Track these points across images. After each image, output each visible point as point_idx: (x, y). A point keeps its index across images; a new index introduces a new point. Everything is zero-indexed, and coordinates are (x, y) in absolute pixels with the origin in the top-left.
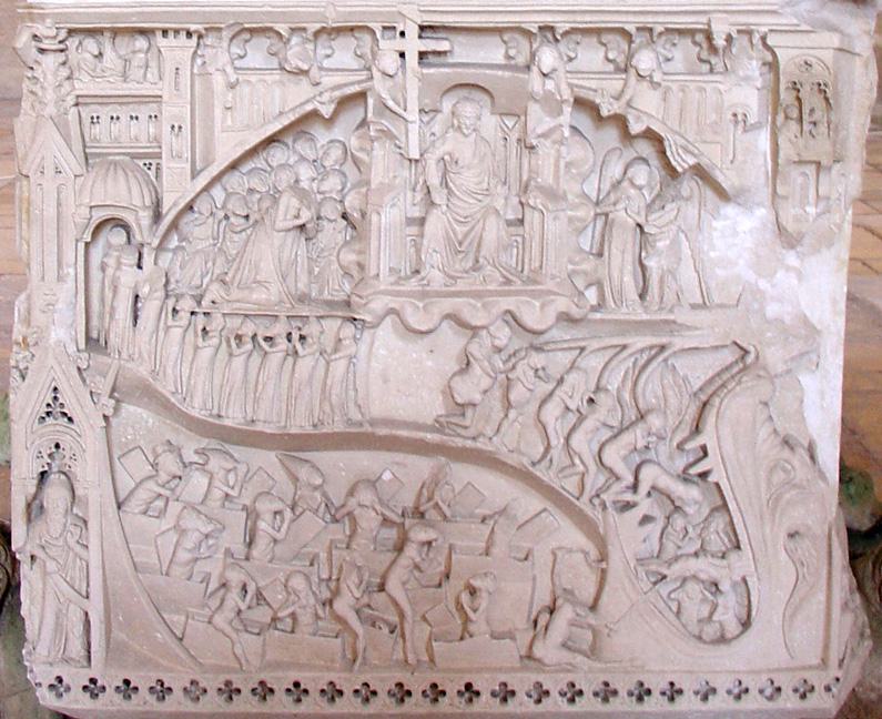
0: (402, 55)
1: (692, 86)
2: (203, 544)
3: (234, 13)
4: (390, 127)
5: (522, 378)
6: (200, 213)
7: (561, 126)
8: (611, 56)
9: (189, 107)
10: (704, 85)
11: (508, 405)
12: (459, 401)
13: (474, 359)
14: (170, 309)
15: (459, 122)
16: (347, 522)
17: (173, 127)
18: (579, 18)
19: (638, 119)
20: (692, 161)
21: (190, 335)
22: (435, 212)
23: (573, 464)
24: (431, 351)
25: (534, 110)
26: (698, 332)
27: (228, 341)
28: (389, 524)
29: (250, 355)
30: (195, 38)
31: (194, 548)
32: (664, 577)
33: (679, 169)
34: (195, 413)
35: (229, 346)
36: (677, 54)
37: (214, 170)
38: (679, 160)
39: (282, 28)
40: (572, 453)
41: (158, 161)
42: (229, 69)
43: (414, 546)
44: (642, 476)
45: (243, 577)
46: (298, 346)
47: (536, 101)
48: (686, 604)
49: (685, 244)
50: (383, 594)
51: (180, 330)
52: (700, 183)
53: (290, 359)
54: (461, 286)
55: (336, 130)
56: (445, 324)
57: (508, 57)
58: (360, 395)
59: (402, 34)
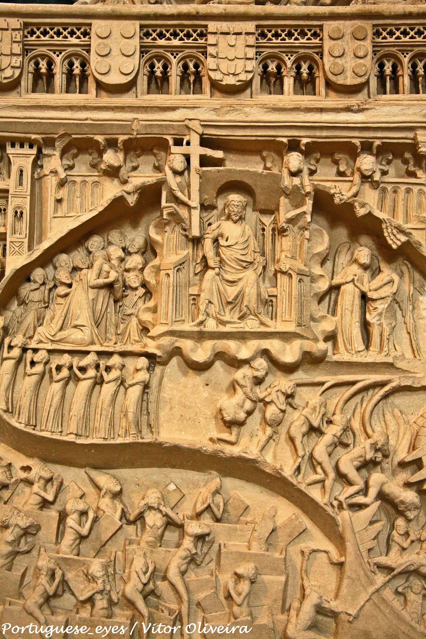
0: (187, 158)
1: (403, 188)
2: (23, 541)
3: (64, 124)
4: (177, 208)
5: (276, 401)
6: (35, 282)
7: (305, 213)
8: (342, 169)
9: (29, 198)
10: (411, 186)
11: (265, 421)
12: (228, 418)
13: (238, 384)
14: (6, 346)
15: (229, 210)
16: (139, 526)
17: (16, 212)
18: (318, 133)
19: (363, 205)
20: (403, 239)
21: (21, 368)
22: (210, 273)
23: (316, 472)
24: (207, 385)
25: (283, 201)
26: (411, 375)
27: (51, 369)
28: (172, 527)
29: (67, 384)
30: (34, 151)
31: (14, 541)
32: (393, 569)
33: (394, 247)
34: (21, 427)
35: (51, 377)
36: (392, 170)
37: (46, 245)
38: (394, 240)
39: (100, 138)
40: (315, 463)
41: (4, 242)
42: (61, 170)
43: (192, 539)
44: (371, 483)
45: (52, 565)
46: (104, 374)
47: (287, 196)
48: (411, 597)
49: (399, 314)
50: (167, 582)
51: (13, 362)
52: (409, 266)
53: (98, 387)
54: (228, 328)
55: (140, 229)
56: (218, 364)
57: (266, 168)
58: (152, 416)
59: (188, 144)
